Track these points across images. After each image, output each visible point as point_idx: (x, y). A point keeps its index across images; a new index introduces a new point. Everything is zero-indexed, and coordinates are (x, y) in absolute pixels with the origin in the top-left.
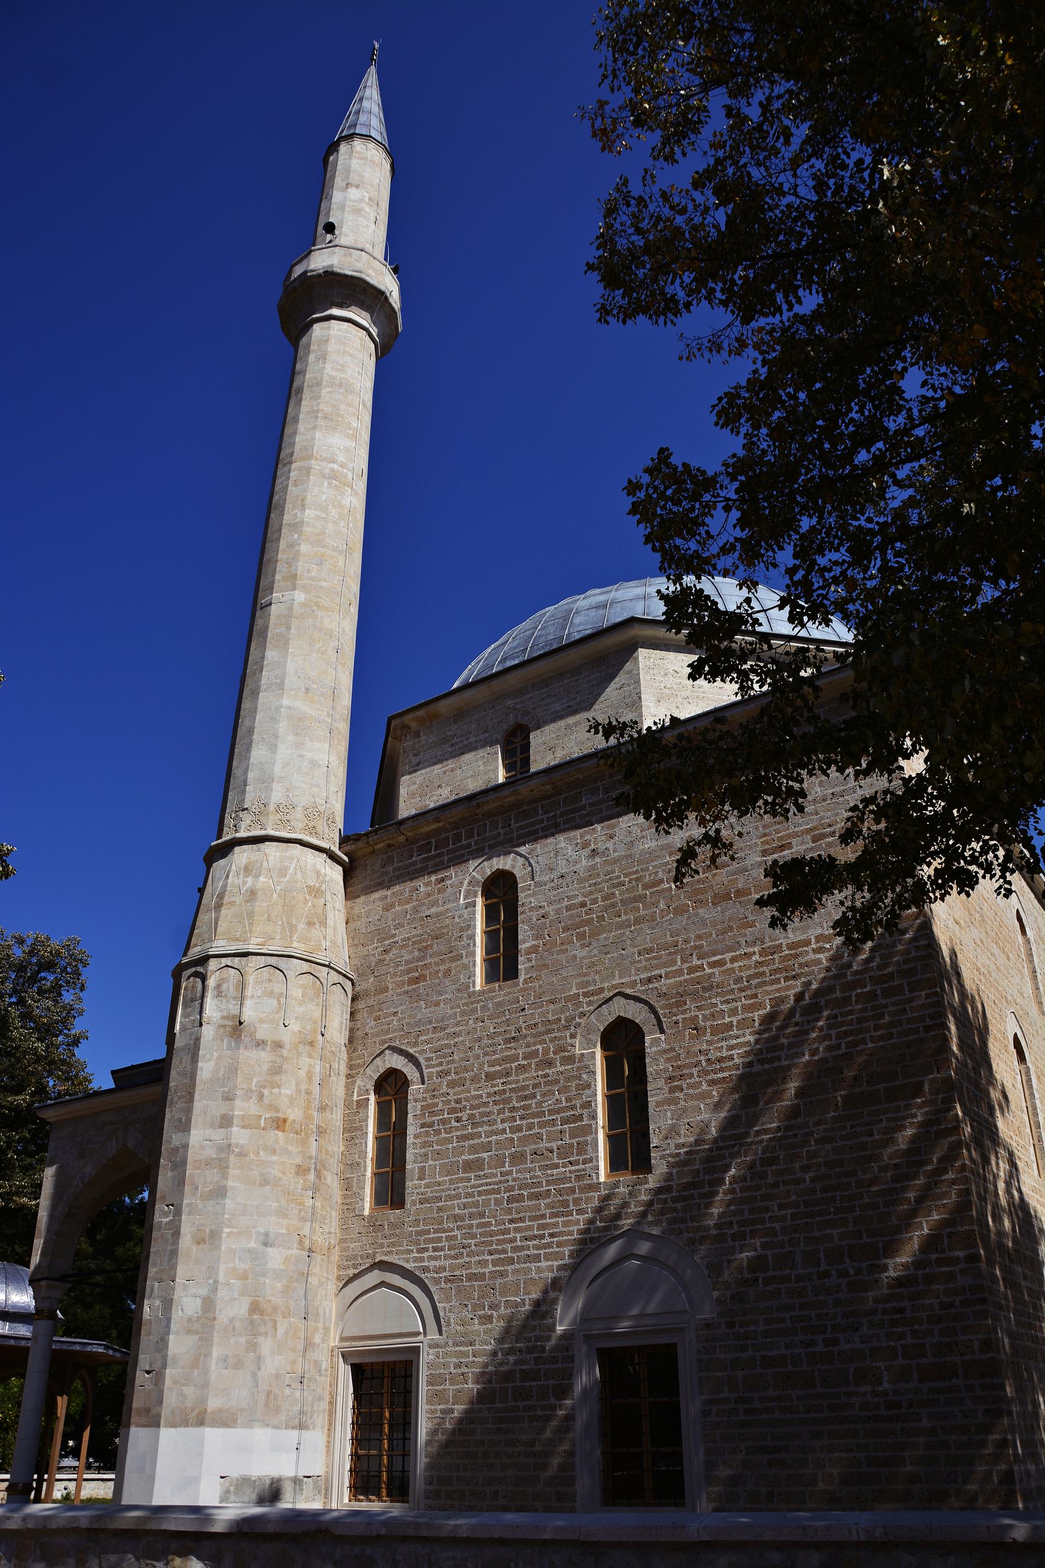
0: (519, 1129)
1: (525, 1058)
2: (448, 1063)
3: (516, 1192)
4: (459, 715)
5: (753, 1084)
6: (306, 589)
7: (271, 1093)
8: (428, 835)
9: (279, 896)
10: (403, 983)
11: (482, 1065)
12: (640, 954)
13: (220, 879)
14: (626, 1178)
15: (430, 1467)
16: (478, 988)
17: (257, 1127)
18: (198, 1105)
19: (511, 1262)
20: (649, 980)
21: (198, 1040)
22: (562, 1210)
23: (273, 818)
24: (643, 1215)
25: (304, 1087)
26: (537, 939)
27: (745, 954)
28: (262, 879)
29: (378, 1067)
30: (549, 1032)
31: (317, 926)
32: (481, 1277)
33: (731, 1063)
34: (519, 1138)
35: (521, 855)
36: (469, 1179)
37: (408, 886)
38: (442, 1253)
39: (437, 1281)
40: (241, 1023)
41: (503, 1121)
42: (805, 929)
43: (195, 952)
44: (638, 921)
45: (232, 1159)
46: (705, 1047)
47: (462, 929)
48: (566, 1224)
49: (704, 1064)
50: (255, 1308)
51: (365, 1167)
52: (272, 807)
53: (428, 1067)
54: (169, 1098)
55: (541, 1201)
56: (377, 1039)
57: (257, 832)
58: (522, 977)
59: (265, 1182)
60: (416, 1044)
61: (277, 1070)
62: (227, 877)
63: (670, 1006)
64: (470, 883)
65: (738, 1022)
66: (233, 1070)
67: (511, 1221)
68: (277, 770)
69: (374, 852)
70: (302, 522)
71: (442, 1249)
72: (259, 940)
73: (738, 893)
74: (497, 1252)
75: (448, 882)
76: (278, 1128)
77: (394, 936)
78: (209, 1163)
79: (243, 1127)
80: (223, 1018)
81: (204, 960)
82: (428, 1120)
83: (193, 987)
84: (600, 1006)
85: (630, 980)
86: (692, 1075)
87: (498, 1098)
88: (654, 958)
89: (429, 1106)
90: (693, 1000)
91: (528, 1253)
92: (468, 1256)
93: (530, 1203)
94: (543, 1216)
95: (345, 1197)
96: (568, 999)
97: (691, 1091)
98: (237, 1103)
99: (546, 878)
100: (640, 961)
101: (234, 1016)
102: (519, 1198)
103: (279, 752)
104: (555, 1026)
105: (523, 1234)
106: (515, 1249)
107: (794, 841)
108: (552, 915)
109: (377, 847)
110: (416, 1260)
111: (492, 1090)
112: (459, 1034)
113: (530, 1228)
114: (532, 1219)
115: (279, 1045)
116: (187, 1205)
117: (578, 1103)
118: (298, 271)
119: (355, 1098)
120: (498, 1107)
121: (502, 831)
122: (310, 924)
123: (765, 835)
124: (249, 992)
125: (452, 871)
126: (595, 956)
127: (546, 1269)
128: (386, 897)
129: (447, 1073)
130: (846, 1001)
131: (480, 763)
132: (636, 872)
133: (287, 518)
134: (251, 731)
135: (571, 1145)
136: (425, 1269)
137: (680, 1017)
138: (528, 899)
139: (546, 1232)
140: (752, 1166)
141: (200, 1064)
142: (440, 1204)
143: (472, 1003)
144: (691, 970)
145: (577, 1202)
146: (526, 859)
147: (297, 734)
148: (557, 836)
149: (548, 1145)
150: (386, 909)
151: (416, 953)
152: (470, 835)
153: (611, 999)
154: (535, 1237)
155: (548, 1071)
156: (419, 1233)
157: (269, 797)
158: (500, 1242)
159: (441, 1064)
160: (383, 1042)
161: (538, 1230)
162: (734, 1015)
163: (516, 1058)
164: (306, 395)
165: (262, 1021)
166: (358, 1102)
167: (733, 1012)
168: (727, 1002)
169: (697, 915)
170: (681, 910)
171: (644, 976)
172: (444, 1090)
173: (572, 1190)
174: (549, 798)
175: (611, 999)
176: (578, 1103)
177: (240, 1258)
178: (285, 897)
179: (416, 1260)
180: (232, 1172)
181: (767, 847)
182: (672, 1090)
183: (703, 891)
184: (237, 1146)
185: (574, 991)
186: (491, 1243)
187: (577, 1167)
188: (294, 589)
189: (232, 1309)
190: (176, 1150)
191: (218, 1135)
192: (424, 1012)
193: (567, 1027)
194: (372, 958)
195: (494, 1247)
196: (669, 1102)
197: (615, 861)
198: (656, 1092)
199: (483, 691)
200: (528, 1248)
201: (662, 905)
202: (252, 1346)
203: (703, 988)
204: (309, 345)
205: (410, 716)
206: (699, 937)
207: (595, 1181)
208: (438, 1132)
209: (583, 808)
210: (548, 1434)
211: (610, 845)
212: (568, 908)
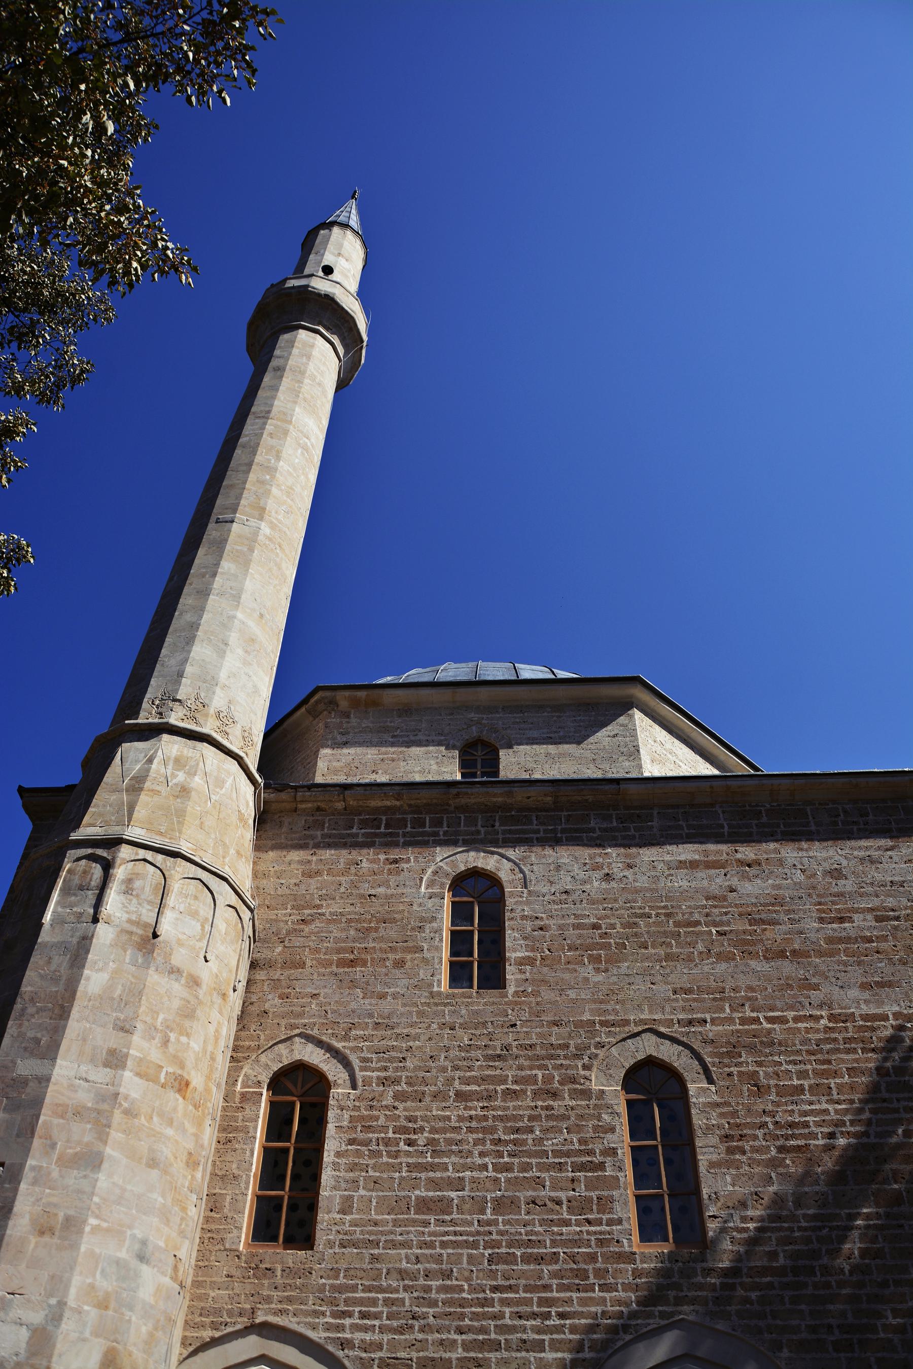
0: (508, 1168)
1: (516, 1082)
2: (396, 1069)
3: (503, 1250)
4: (406, 710)
6: (273, 527)
7: (178, 1040)
8: (377, 810)
9: (214, 807)
10: (329, 963)
11: (449, 1081)
12: (675, 992)
13: (137, 761)
17: (155, 1080)
18: (74, 1026)
20: (690, 1023)
21: (85, 943)
22: (578, 1279)
25: (210, 1048)
26: (533, 951)
27: (811, 1016)
28: (197, 779)
29: (280, 1056)
30: (552, 1057)
33: (807, 1131)
34: (508, 1180)
36: (427, 1224)
37: (343, 856)
38: (377, 1323)
40: (155, 936)
41: (482, 1154)
42: (880, 1003)
44: (669, 957)
45: (117, 1116)
46: (770, 1107)
47: (422, 920)
48: (583, 1302)
49: (771, 1126)
51: (248, 1183)
52: (212, 711)
53: (363, 1069)
54: (18, 1007)
55: (544, 1267)
56: (283, 1022)
58: (511, 989)
59: (153, 1163)
60: (346, 1038)
61: (188, 1013)
62: (150, 761)
63: (721, 1055)
64: (435, 873)
65: (810, 1086)
66: (136, 993)
67: (495, 1289)
68: (223, 676)
69: (295, 810)
70: (276, 470)
71: (377, 1316)
73: (794, 952)
74: (470, 1329)
75: (405, 866)
76: (179, 1091)
77: (319, 907)
78: (79, 1113)
79: (138, 1074)
80: (129, 921)
81: (115, 842)
82: (361, 1136)
83: (85, 872)
84: (624, 1040)
85: (670, 1015)
86: (755, 1137)
87: (474, 1124)
88: (695, 1000)
89: (363, 1118)
90: (749, 1053)
91: (525, 1337)
92: (422, 1330)
93: (525, 1267)
94: (547, 1288)
95: (207, 1220)
96: (579, 1024)
97: (757, 1156)
98: (136, 1038)
99: (545, 890)
100: (676, 1000)
101: (146, 925)
102: (509, 1259)
103: (226, 658)
104: (559, 1052)
105: (516, 1309)
106: (501, 1329)
107: (856, 917)
108: (554, 931)
110: (328, 1327)
111: (467, 1114)
112: (417, 1038)
113: (528, 1302)
114: (527, 1288)
115: (195, 982)
116: (33, 1168)
117: (598, 1147)
119: (238, 1088)
120: (475, 1136)
121: (482, 830)
122: (238, 853)
123: (820, 904)
124: (171, 900)
125: (410, 853)
128: (309, 862)
129: (396, 1081)
132: (665, 907)
134: (194, 627)
135: (590, 1199)
138: (516, 904)
139: (553, 1311)
141: (86, 972)
142: (376, 1251)
143: (436, 1004)
144: (743, 1021)
145: (598, 1273)
146: (515, 863)
147: (246, 652)
148: (557, 848)
149: (553, 1194)
150: (309, 875)
151: (352, 932)
152: (438, 823)
153: (638, 1034)
154: (534, 1316)
155: (551, 1103)
156: (340, 1289)
157: (211, 700)
158: (475, 1316)
159: (385, 1069)
160: (293, 1027)
161: (539, 1305)
162: (804, 1078)
163: (504, 1081)
165: (180, 943)
166: (243, 1096)
167: (802, 1075)
168: (794, 1063)
169: (747, 965)
170: (724, 957)
172: (388, 1100)
173: (593, 1258)
175: (638, 1034)
176: (598, 1147)
177: (103, 1271)
179: (328, 1327)
180: (115, 1135)
181: (823, 915)
182: (730, 1151)
183: (753, 943)
184: (126, 1098)
185: (586, 1017)
186: (462, 1317)
187: (598, 1228)
188: (261, 518)
191: (101, 1075)
192: (359, 1002)
193: (578, 1056)
195: (467, 1322)
196: (729, 1164)
197: (637, 891)
198: (708, 1150)
199: (448, 692)
200: (524, 1330)
201: (700, 947)
203: (762, 1042)
205: (347, 693)
206: (750, 988)
207: (627, 1249)
208: (378, 1154)
212: (576, 927)
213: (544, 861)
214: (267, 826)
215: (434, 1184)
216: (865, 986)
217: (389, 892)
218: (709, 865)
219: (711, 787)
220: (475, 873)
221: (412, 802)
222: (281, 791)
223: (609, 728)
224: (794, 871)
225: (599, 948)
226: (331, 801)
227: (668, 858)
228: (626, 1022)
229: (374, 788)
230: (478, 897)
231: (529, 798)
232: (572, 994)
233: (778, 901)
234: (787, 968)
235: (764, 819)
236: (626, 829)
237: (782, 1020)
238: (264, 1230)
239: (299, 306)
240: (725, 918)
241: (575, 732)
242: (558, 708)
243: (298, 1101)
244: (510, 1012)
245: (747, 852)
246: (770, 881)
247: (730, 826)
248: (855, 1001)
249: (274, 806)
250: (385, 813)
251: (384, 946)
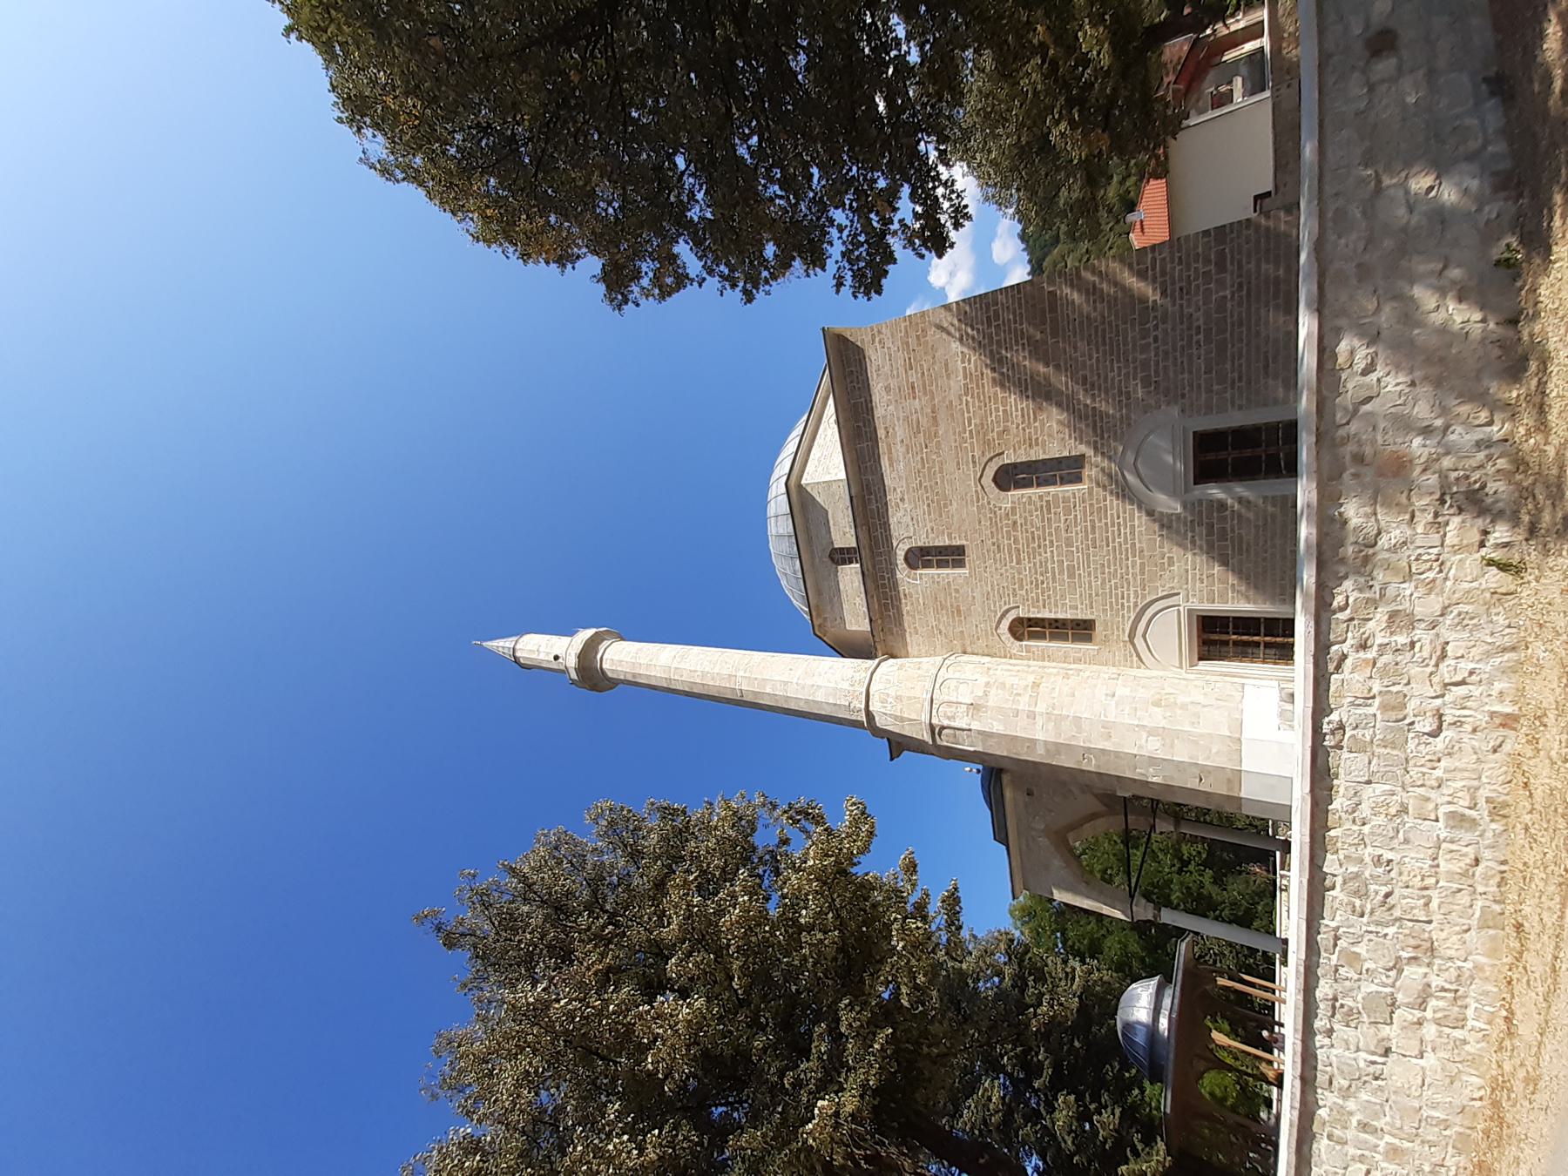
4: (819, 593)
5: (1040, 392)
14: (1086, 472)
15: (1273, 602)
19: (1133, 545)
21: (979, 732)
23: (857, 687)
24: (1110, 458)
32: (1142, 564)
39: (1144, 597)
43: (927, 738)
44: (941, 471)
50: (1157, 704)
58: (964, 542)
85: (972, 472)
102: (1094, 540)
115: (988, 684)
118: (574, 675)
127: (1140, 520)
130: (998, 342)
134: (807, 701)
136: (1136, 605)
140: (1086, 390)
167: (997, 410)
178: (901, 690)
189: (1157, 717)
190: (1047, 751)
191: (1039, 721)
192: (978, 607)
202: (1184, 707)
210: (1251, 515)
215: (1061, 572)
216: (948, 376)
218: (890, 452)
220: (906, 559)
225: (939, 505)
230: (921, 557)
234: (941, 416)
237: (970, 420)
238: (1088, 638)
242: (806, 520)
243: (1026, 628)
245: (881, 433)
248: (957, 382)
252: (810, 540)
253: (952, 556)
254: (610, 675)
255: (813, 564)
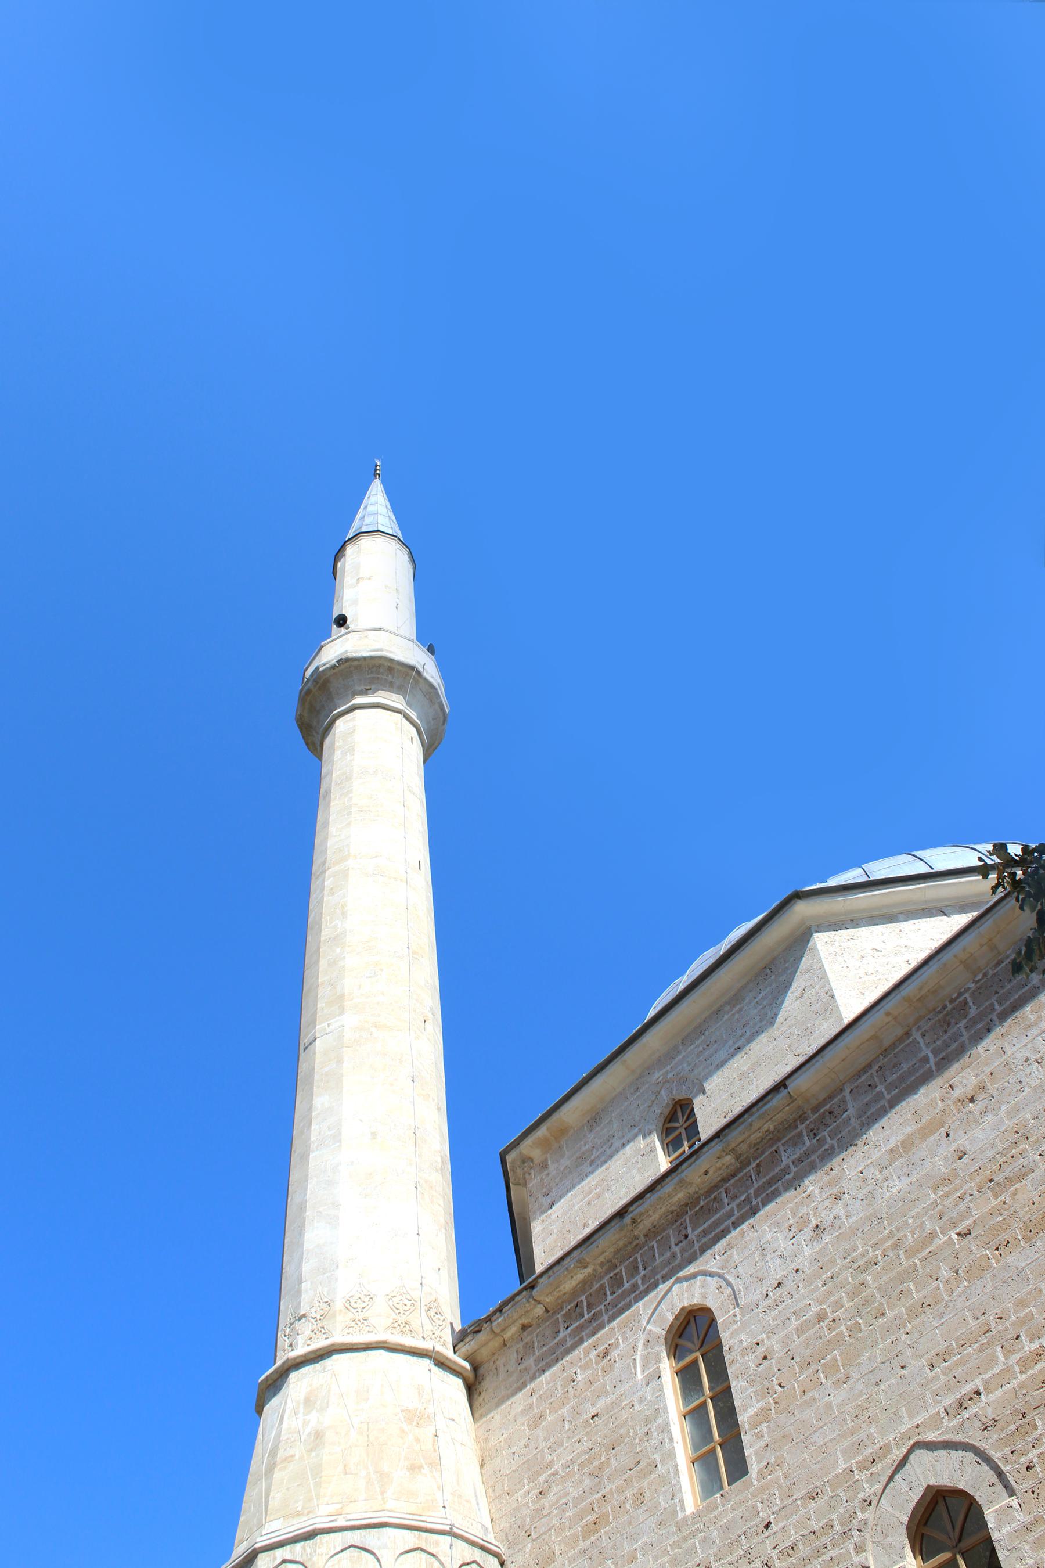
4: (594, 1119)
8: (575, 1293)
10: (575, 1538)
16: (690, 1508)
31: (426, 1470)
35: (711, 1275)
44: (913, 1313)
47: (647, 1421)
52: (338, 1305)
57: (320, 1343)
58: (754, 1468)
72: (332, 1509)
75: (615, 1354)
77: (550, 1464)
84: (891, 1478)
88: (957, 1364)
99: (756, 1296)
100: (936, 1378)
104: (825, 1539)
108: (779, 1351)
109: (507, 1335)
121: (677, 1250)
126: (861, 1394)
128: (531, 1406)
131: (634, 1172)
132: (891, 1235)
133: (326, 933)
134: (302, 1208)
137: (1033, 1455)
143: (685, 1539)
146: (720, 1276)
150: (534, 1426)
151: (587, 1482)
152: (634, 1270)
164: (335, 794)
171: (950, 1400)
174: (734, 1175)
185: (842, 1465)
194: (525, 1511)
201: (945, 1273)
204: (333, 743)
205: (529, 1141)
206: (1021, 1303)
209: (786, 1171)
211: (839, 1209)
212: (800, 1331)
213: (747, 1252)
214: (486, 1384)
217: (609, 1400)
218: (924, 1133)
219: (888, 1014)
221: (602, 1259)
222: (479, 1331)
223: (794, 986)
224: (1028, 1070)
226: (527, 1312)
227: (876, 1155)
228: (886, 1449)
229: (555, 1269)
231: (706, 1173)
232: (818, 1439)
233: (1021, 1134)
235: (973, 1011)
236: (821, 1142)
239: (317, 706)
240: (962, 1207)
241: (761, 1020)
242: (735, 999)
244: (760, 1506)
246: (1003, 1108)
247: (935, 1053)
249: (485, 1353)
250: (583, 1291)
251: (619, 1482)
252: (697, 1030)
253: (724, 1452)
254: (327, 742)
255: (648, 1069)
